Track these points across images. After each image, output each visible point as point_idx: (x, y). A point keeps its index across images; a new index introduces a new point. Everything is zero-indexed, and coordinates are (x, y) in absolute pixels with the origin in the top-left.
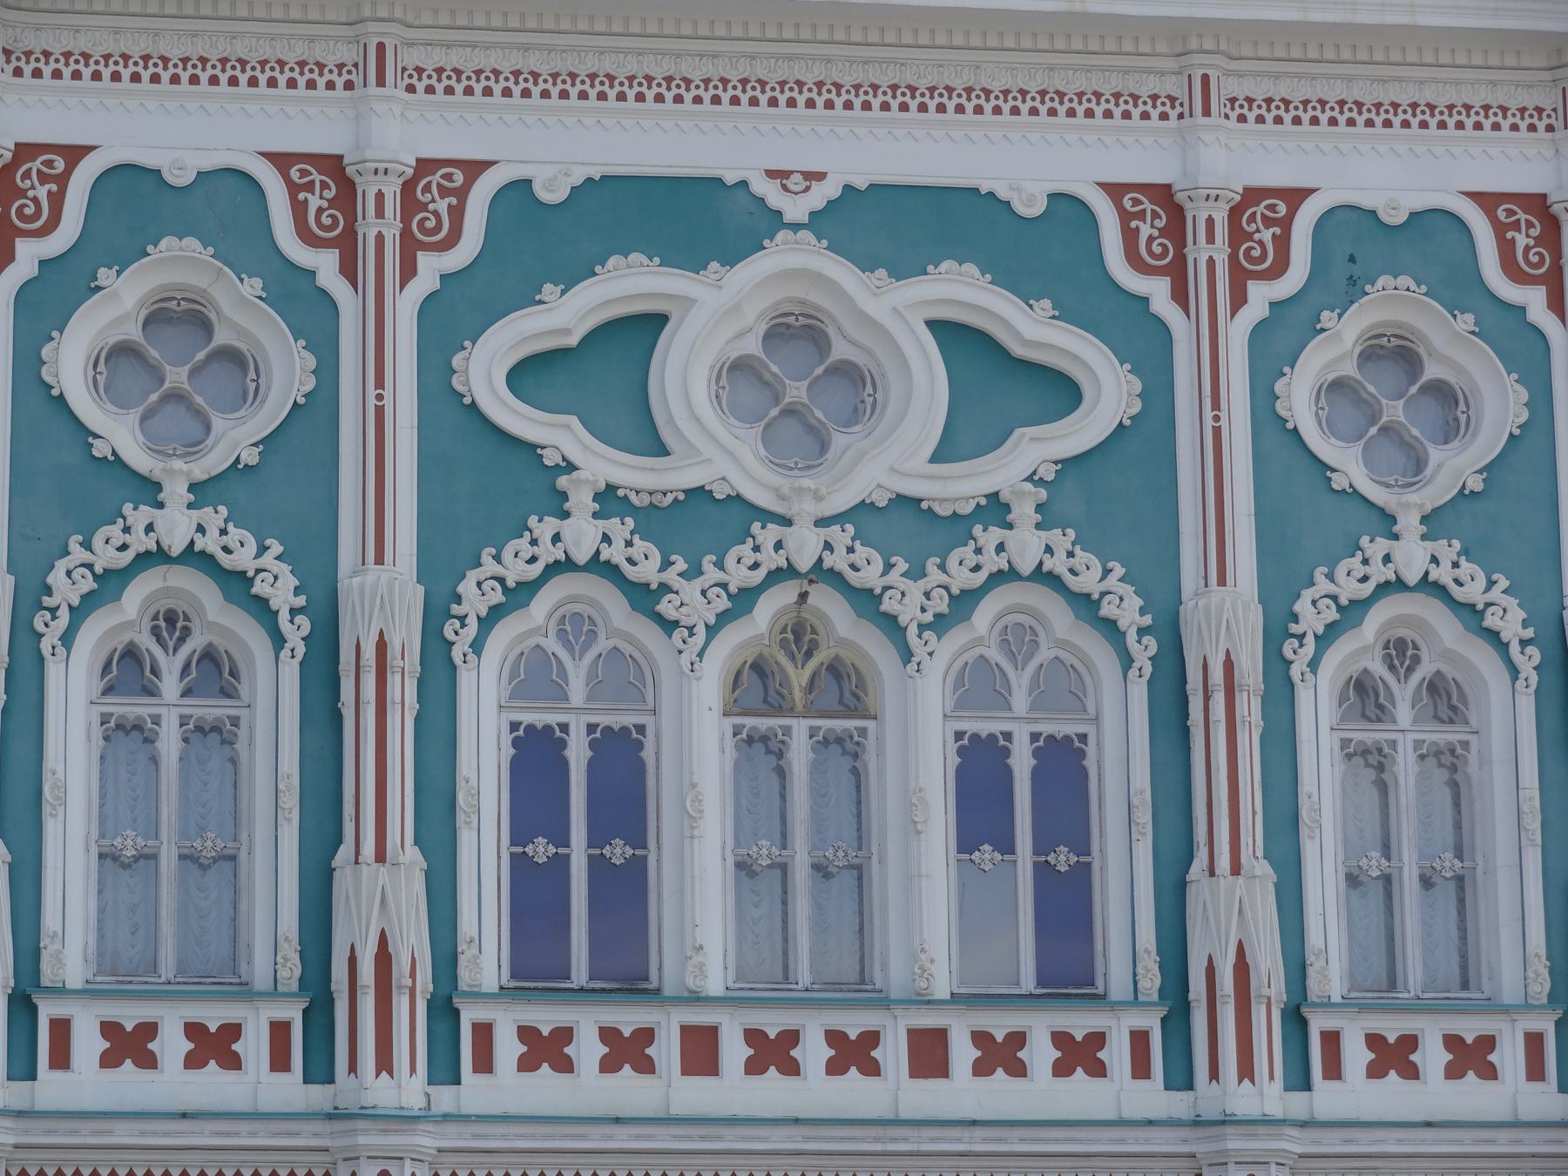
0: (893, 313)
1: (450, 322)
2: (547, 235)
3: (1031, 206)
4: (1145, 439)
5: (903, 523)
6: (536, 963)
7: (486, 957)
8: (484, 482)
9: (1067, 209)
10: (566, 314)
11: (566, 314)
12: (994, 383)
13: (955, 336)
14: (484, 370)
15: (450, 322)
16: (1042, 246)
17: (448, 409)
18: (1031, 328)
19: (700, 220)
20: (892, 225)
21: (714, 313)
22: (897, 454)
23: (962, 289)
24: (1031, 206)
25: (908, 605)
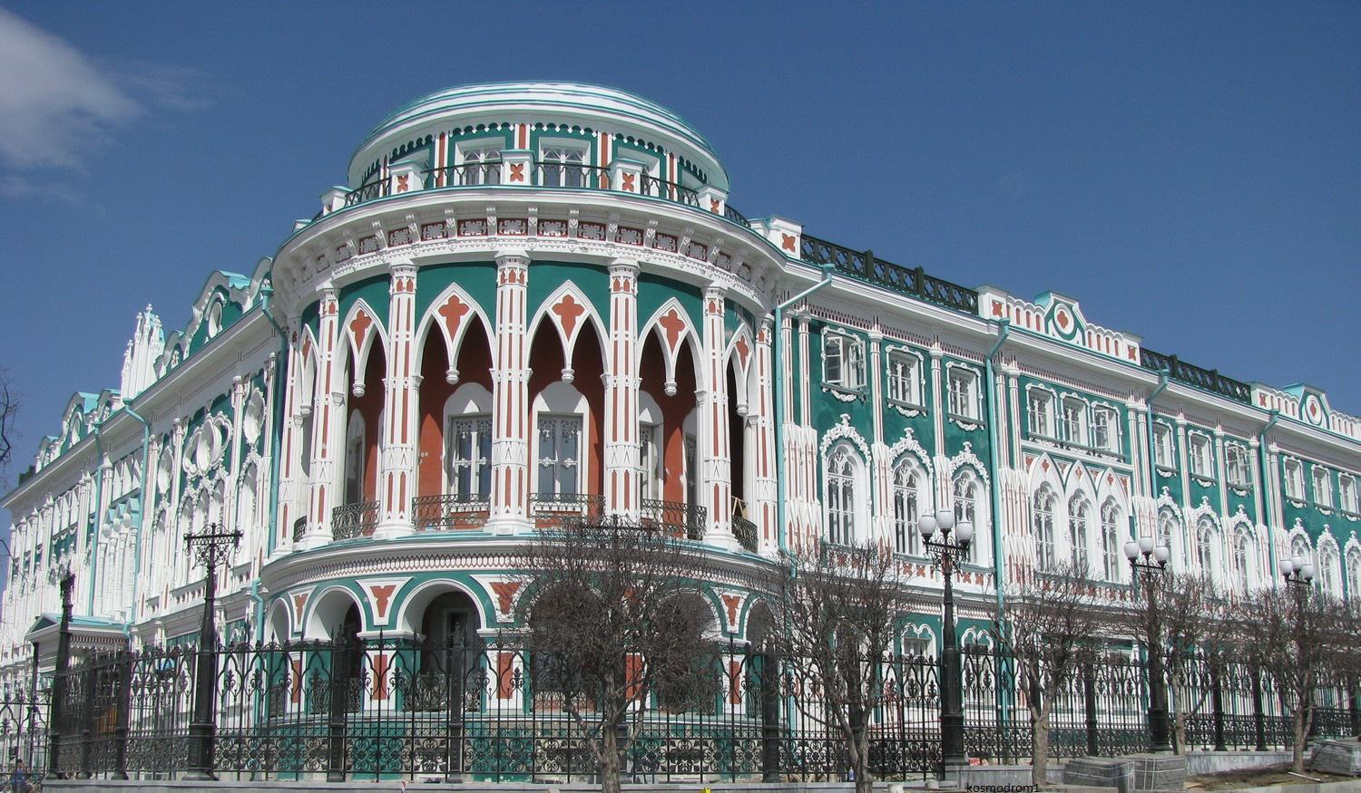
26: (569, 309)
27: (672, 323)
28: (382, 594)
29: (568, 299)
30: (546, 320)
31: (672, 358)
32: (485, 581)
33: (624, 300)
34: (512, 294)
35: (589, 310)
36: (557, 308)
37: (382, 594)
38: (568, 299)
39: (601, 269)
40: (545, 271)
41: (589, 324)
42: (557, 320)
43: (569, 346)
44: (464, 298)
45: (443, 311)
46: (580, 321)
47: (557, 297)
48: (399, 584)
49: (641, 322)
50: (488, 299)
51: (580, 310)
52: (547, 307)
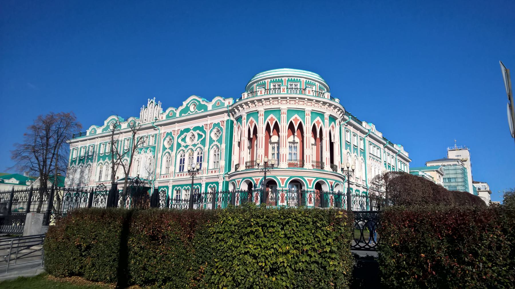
0: (195, 133)
1: (178, 138)
2: (182, 132)
3: (201, 126)
4: (205, 138)
5: (194, 145)
6: (180, 170)
7: (178, 170)
8: (179, 145)
9: (203, 126)
10: (183, 136)
11: (183, 136)
12: (200, 136)
13: (198, 134)
14: (180, 141)
15: (178, 138)
16: (201, 129)
17: (178, 142)
18: (201, 133)
19: (187, 130)
20: (195, 129)
21: (189, 135)
22: (196, 141)
23: (198, 131)
24: (201, 126)
25: (194, 149)
26: (272, 119)
27: (296, 120)
28: (238, 182)
29: (272, 117)
30: (268, 124)
31: (296, 128)
32: (254, 178)
33: (284, 117)
34: (261, 118)
35: (276, 120)
36: (269, 120)
37: (238, 182)
38: (272, 117)
39: (279, 110)
40: (267, 112)
41: (276, 122)
42: (269, 122)
43: (272, 128)
44: (253, 120)
45: (250, 123)
46: (274, 122)
47: (269, 117)
48: (241, 180)
49: (288, 120)
50: (257, 119)
51: (274, 119)
52: (267, 120)
